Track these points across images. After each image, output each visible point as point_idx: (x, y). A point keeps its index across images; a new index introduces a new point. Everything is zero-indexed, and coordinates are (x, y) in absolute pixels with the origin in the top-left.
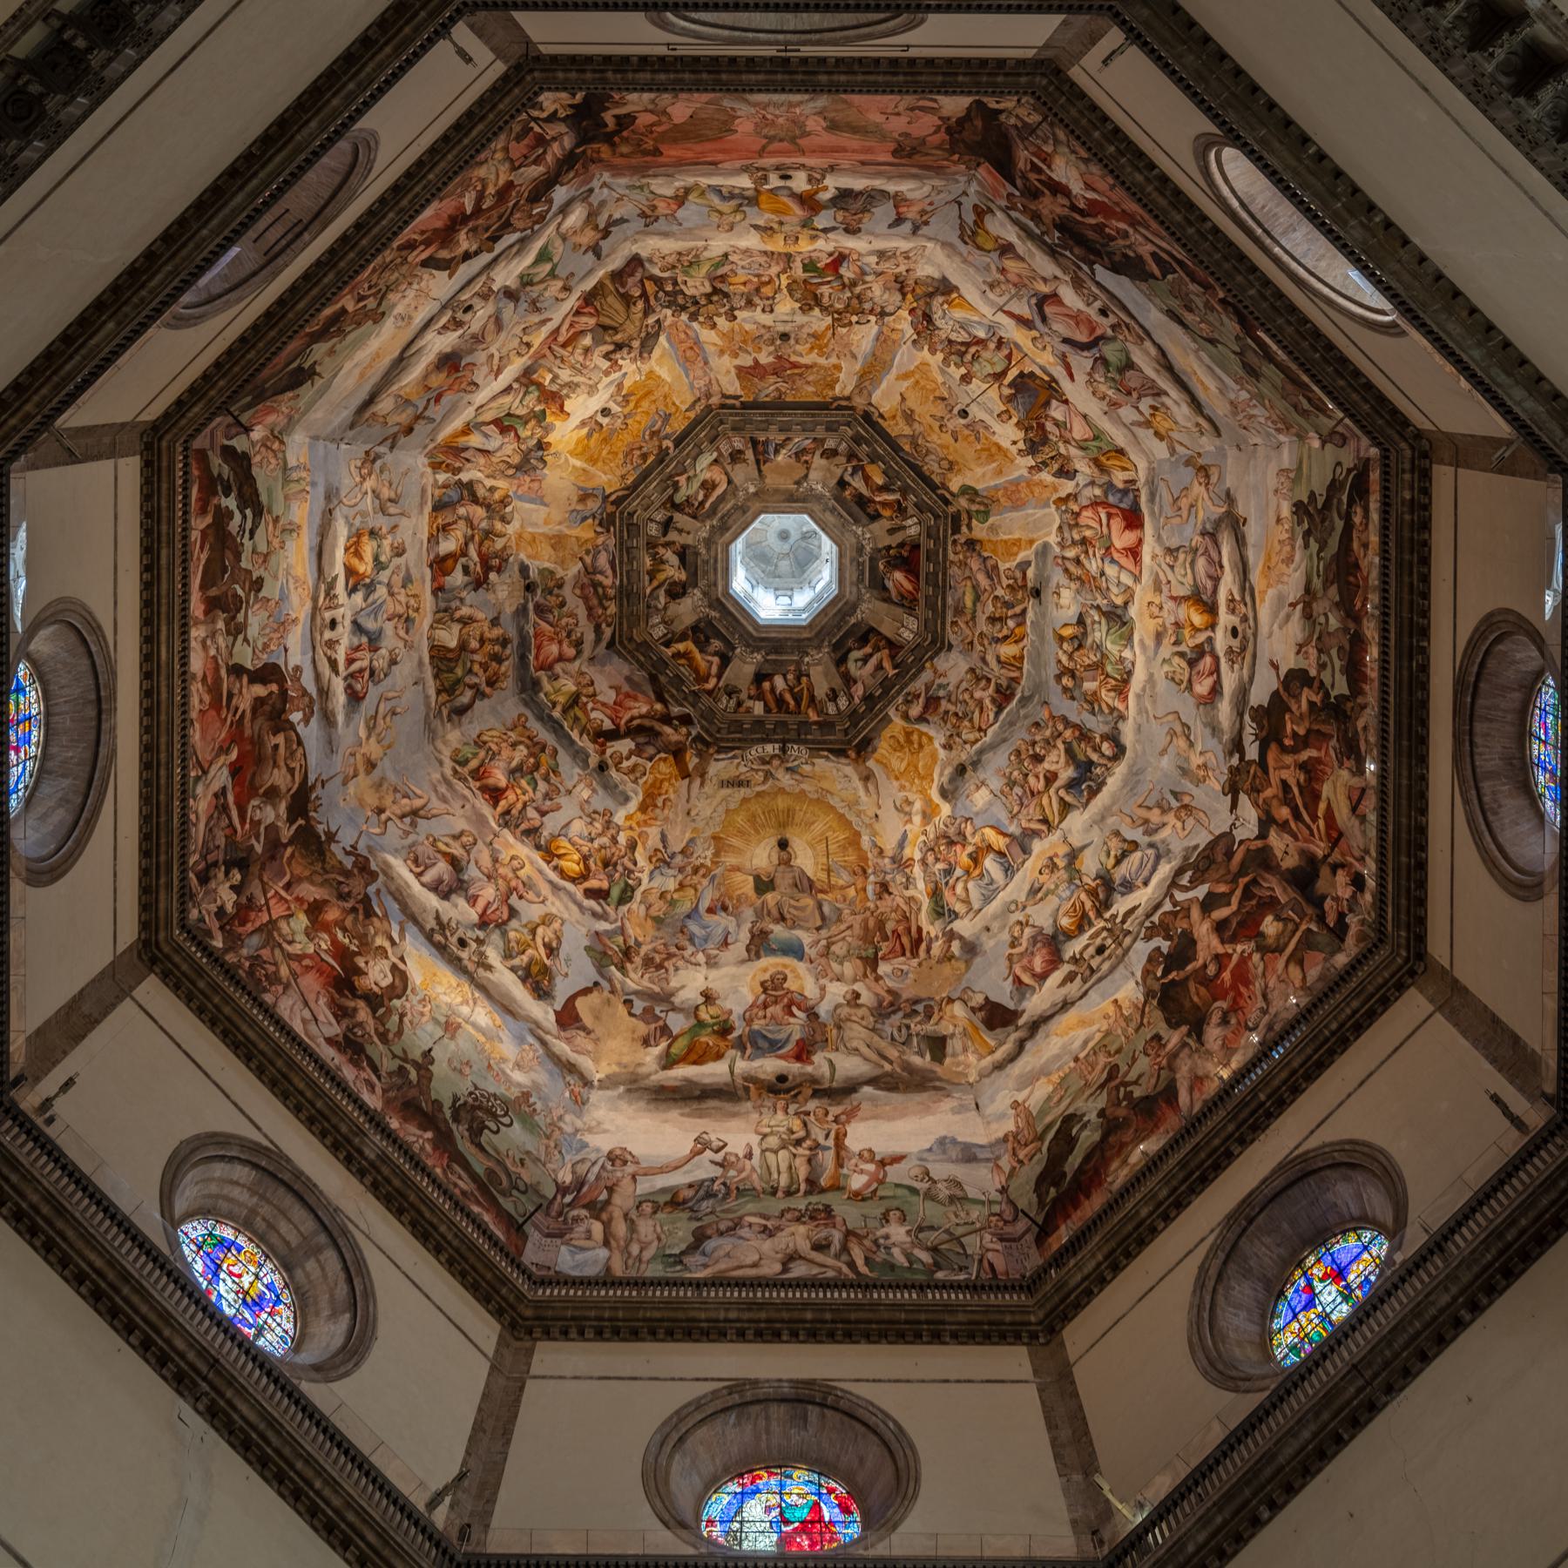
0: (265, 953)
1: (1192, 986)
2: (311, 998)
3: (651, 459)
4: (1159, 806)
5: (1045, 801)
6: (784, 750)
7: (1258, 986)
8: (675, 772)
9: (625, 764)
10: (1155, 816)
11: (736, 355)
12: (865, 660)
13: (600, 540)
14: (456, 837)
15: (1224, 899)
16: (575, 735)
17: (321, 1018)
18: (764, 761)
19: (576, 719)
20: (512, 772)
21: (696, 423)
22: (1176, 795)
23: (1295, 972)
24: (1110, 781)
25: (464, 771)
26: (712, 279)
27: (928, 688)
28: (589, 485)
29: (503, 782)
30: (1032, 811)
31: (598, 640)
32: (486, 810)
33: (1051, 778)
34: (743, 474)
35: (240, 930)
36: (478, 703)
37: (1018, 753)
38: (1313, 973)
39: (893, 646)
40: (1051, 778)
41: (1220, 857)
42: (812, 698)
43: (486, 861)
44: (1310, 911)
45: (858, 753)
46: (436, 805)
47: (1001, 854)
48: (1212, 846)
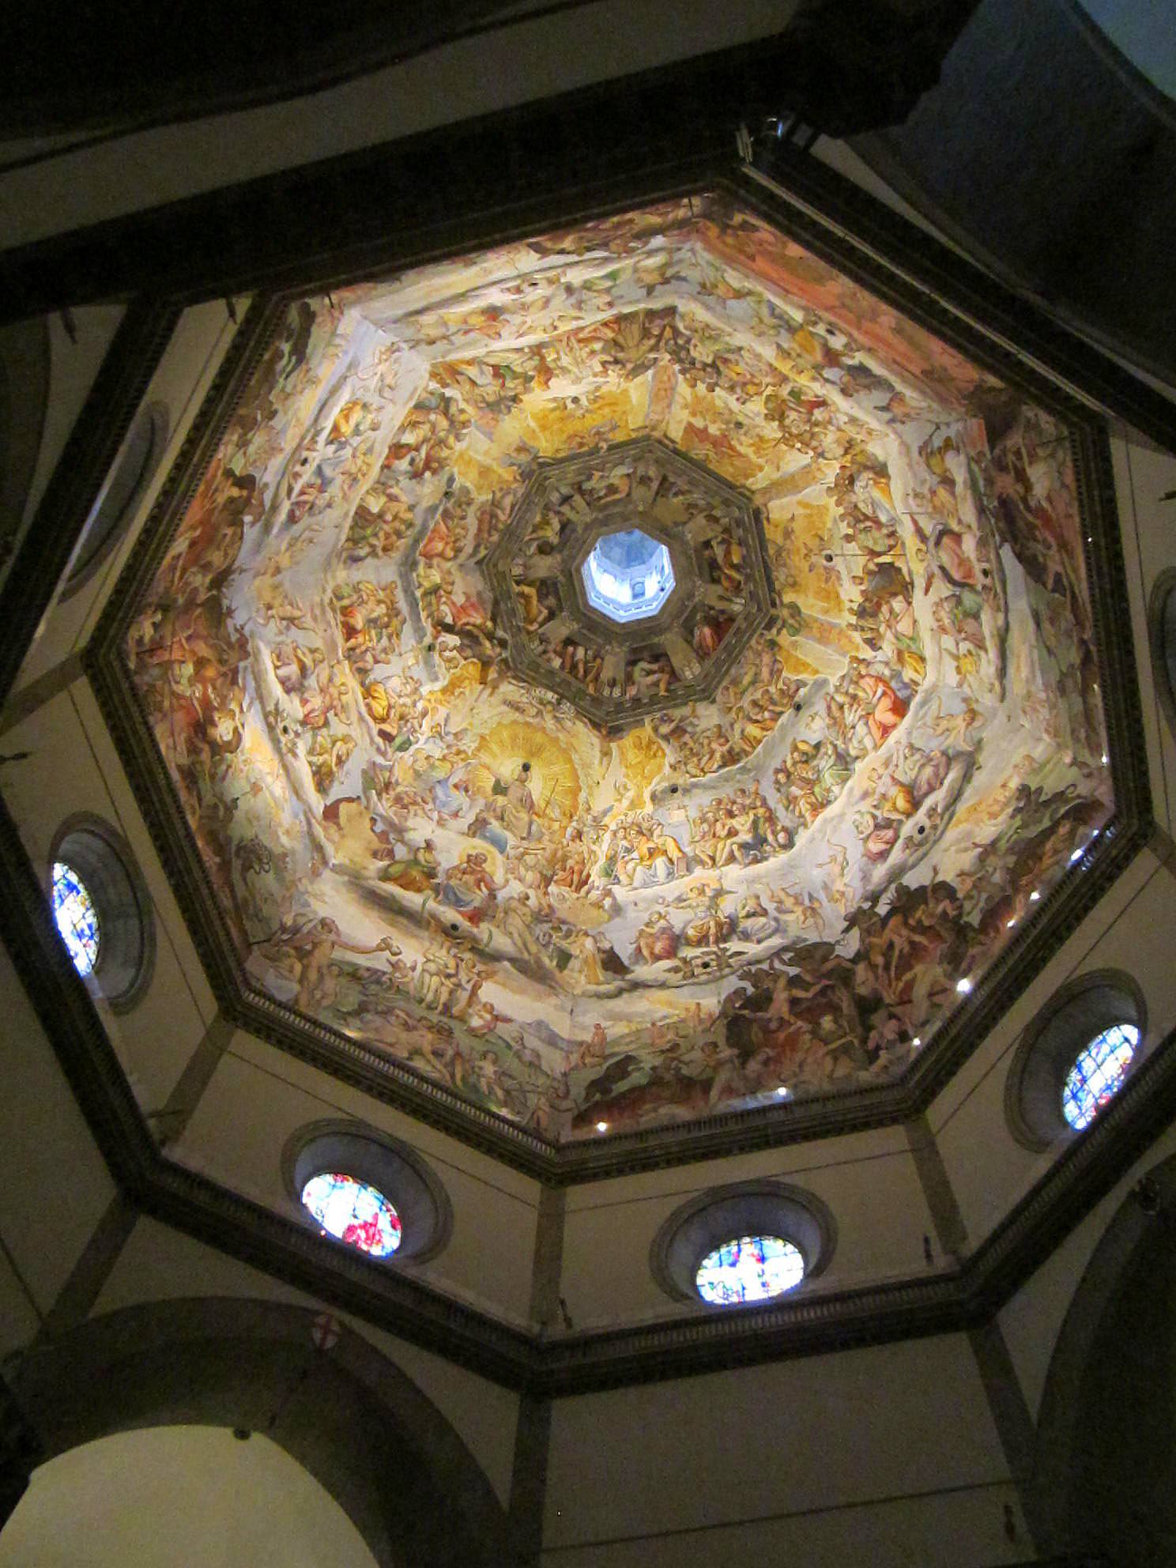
0: (159, 683)
1: (755, 1028)
2: (177, 729)
3: (585, 449)
5: (720, 846)
7: (799, 1056)
8: (478, 676)
9: (447, 654)
10: (789, 903)
11: (694, 414)
12: (649, 673)
13: (514, 486)
14: (313, 651)
16: (423, 615)
18: (541, 702)
19: (430, 604)
21: (634, 441)
22: (811, 898)
23: (829, 1060)
24: (772, 860)
26: (717, 357)
28: (531, 443)
29: (359, 625)
31: (472, 556)
36: (369, 560)
37: (720, 802)
38: (840, 1072)
40: (732, 833)
42: (596, 678)
43: (324, 679)
44: (859, 1030)
45: (609, 733)
46: (308, 621)
47: (671, 861)
48: (816, 945)
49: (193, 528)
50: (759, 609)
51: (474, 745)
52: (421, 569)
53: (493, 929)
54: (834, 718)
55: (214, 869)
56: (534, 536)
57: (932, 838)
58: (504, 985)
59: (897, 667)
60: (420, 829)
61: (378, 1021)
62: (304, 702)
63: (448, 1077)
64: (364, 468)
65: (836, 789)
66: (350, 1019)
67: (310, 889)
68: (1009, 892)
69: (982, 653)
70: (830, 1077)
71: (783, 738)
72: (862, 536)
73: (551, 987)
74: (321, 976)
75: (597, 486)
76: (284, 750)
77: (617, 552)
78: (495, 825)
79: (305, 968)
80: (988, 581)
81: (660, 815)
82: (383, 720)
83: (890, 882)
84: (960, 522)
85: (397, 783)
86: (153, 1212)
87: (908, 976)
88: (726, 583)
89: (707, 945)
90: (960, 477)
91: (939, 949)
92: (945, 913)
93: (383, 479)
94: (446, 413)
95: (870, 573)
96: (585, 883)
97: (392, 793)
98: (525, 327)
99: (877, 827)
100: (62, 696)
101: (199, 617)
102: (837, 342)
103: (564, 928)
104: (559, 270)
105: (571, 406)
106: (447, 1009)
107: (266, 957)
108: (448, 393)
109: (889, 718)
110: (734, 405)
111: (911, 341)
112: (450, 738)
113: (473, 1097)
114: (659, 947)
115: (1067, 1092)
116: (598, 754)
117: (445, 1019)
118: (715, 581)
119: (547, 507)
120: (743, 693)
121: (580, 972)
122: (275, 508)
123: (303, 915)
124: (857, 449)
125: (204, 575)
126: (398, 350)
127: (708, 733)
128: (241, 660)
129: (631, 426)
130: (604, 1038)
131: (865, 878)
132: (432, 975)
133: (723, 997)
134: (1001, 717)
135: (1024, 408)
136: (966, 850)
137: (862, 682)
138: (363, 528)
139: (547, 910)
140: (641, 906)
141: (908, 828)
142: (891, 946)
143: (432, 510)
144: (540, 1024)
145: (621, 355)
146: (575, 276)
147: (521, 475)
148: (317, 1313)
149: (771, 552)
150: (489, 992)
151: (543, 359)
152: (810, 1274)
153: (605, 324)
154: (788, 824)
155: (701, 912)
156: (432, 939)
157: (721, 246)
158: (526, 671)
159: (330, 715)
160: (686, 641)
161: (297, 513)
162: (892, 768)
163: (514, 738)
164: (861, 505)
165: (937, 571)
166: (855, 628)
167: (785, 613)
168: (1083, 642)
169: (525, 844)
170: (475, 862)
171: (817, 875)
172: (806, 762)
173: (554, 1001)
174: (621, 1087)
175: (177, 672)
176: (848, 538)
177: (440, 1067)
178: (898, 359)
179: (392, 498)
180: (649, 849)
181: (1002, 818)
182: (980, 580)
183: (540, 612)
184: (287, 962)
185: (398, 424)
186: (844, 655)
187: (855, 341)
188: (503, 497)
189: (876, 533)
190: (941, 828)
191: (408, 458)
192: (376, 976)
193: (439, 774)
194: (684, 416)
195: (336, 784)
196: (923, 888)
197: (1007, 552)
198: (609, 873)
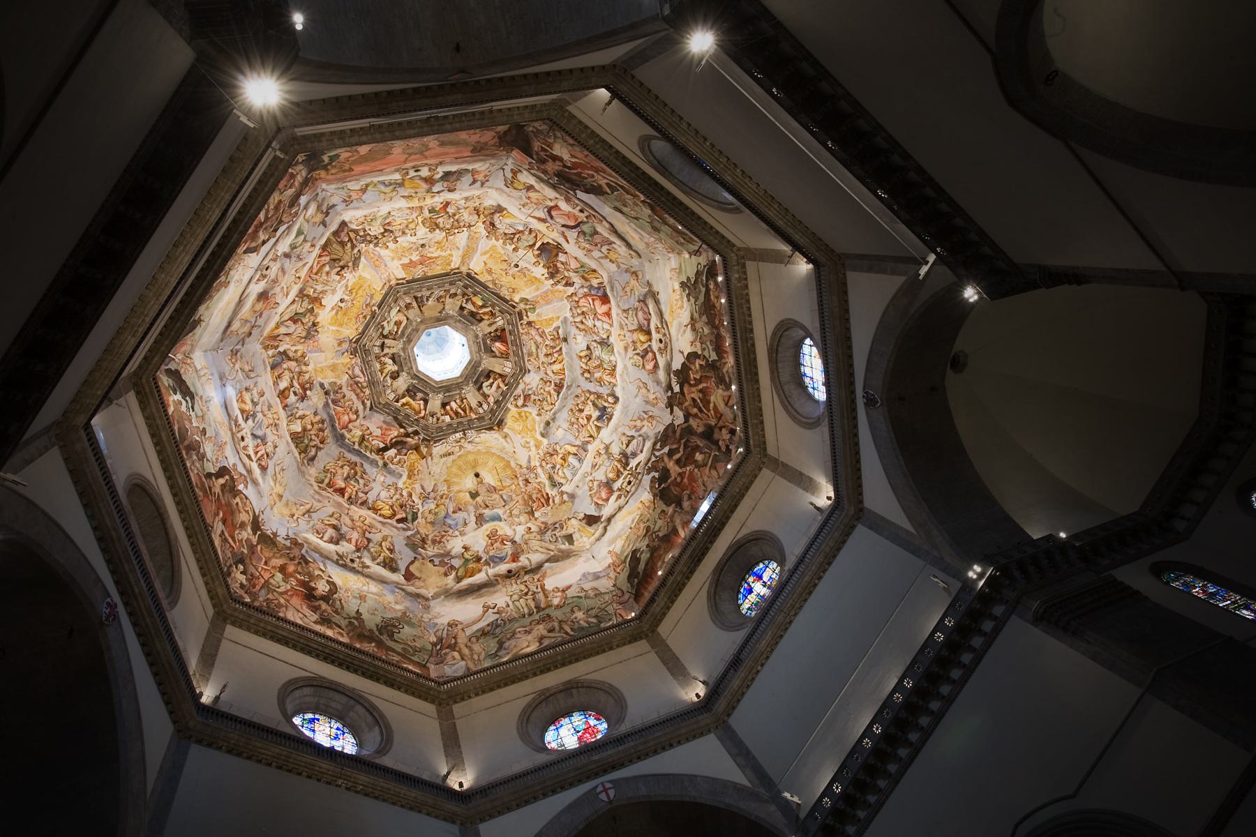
0: (270, 596)
2: (299, 608)
3: (368, 317)
4: (639, 419)
5: (589, 428)
6: (465, 434)
7: (700, 481)
9: (395, 460)
10: (639, 423)
11: (400, 259)
12: (491, 385)
13: (353, 362)
14: (332, 516)
15: (677, 450)
16: (368, 454)
17: (307, 614)
19: (366, 447)
20: (346, 479)
22: (645, 412)
23: (714, 473)
25: (324, 485)
26: (383, 226)
27: (523, 392)
29: (343, 485)
30: (584, 433)
32: (340, 500)
33: (589, 418)
34: (413, 313)
35: (254, 590)
37: (572, 410)
38: (721, 472)
39: (501, 376)
41: (670, 434)
42: (471, 408)
44: (713, 447)
45: (499, 427)
49: (218, 514)
50: (510, 314)
51: (445, 488)
52: (347, 435)
53: (527, 556)
54: (584, 330)
55: (375, 650)
56: (384, 375)
57: (668, 340)
58: (554, 574)
59: (588, 283)
60: (455, 545)
61: (513, 642)
62: (349, 541)
63: (565, 636)
64: (275, 416)
65: (612, 358)
66: (499, 654)
67: (430, 616)
68: (716, 332)
69: (614, 245)
70: (719, 477)
71: (572, 359)
72: (520, 243)
73: (574, 555)
74: (471, 649)
75: (390, 328)
76: (360, 569)
77: (432, 348)
78: (487, 512)
79: (460, 652)
80: (586, 214)
81: (554, 439)
82: (394, 515)
83: (669, 375)
84: (551, 200)
85: (427, 536)
86: (482, 820)
87: (712, 405)
88: (486, 317)
89: (622, 474)
90: (532, 181)
91: (711, 384)
92: (701, 365)
93: (289, 413)
94: (290, 359)
95: (539, 256)
96: (549, 498)
97: (428, 542)
98: (285, 289)
99: (643, 357)
100: (224, 644)
101: (261, 548)
102: (425, 172)
103: (557, 526)
104: (273, 251)
105: (342, 305)
106: (538, 607)
107: (436, 664)
108: (281, 349)
109: (605, 308)
110: (413, 239)
111: (452, 143)
112: (432, 494)
113: (584, 633)
114: (604, 495)
115: (811, 390)
116: (503, 440)
117: (541, 614)
118: (481, 320)
119: (377, 357)
120: (538, 356)
121: (581, 537)
122: (250, 471)
123: (438, 630)
124: (482, 209)
125: (245, 530)
126: (237, 351)
127: (540, 387)
128: (301, 550)
129: (379, 289)
130: (616, 554)
131: (658, 383)
132: (518, 601)
133: (648, 488)
134: (647, 265)
135: (526, 128)
136: (685, 331)
137: (580, 304)
138: (302, 442)
139: (543, 526)
140: (580, 485)
141: (655, 346)
142: (693, 400)
143: (326, 405)
144: (584, 575)
145: (342, 263)
146: (283, 247)
147: (351, 354)
148: (597, 787)
149: (491, 286)
150: (550, 584)
151: (308, 296)
152: (781, 563)
153: (320, 256)
154: (608, 392)
155: (607, 463)
156: (504, 586)
157: (330, 177)
158: (435, 435)
159: (367, 535)
160: (494, 357)
161: (263, 463)
162: (625, 327)
163: (460, 468)
164: (507, 231)
165: (564, 229)
166: (556, 284)
167: (522, 306)
168: (643, 202)
169: (507, 507)
170: (492, 536)
171: (638, 400)
172: (590, 359)
173: (581, 560)
174: (642, 566)
175: (274, 583)
176: (515, 250)
177: (557, 635)
178: (456, 156)
179: (302, 417)
180: (561, 458)
181: (686, 304)
182: (582, 216)
183: (420, 404)
184: (449, 657)
185: (271, 383)
186: (562, 300)
187: (431, 165)
188: (353, 370)
189: (523, 237)
190: (667, 333)
191: (291, 393)
192: (494, 625)
193: (443, 514)
194: (397, 263)
195: (399, 562)
196: (683, 364)
197: (580, 194)
198: (554, 484)
